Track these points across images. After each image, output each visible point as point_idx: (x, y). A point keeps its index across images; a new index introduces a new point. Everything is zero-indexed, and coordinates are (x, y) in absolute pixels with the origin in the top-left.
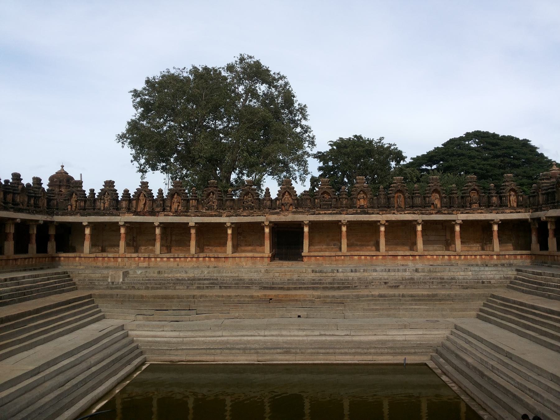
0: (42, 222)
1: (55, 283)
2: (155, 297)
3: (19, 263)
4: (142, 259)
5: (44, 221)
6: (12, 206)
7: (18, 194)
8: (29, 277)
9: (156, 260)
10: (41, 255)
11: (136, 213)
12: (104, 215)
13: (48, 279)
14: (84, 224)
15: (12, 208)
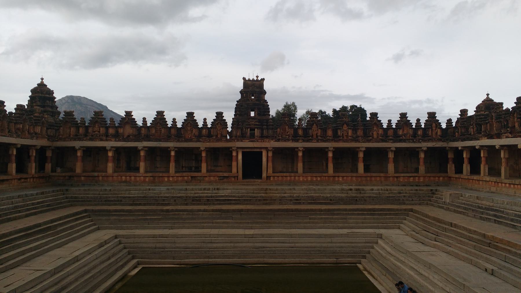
0: (425, 149)
1: (404, 196)
2: (435, 219)
3: (401, 179)
4: (493, 183)
5: (428, 148)
6: (393, 138)
7: (400, 129)
8: (378, 190)
9: (502, 185)
10: (429, 175)
11: (491, 137)
12: (471, 140)
13: (400, 193)
14: (460, 148)
15: (391, 140)
